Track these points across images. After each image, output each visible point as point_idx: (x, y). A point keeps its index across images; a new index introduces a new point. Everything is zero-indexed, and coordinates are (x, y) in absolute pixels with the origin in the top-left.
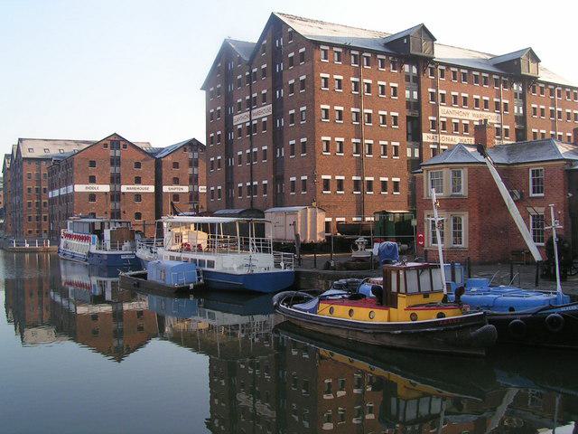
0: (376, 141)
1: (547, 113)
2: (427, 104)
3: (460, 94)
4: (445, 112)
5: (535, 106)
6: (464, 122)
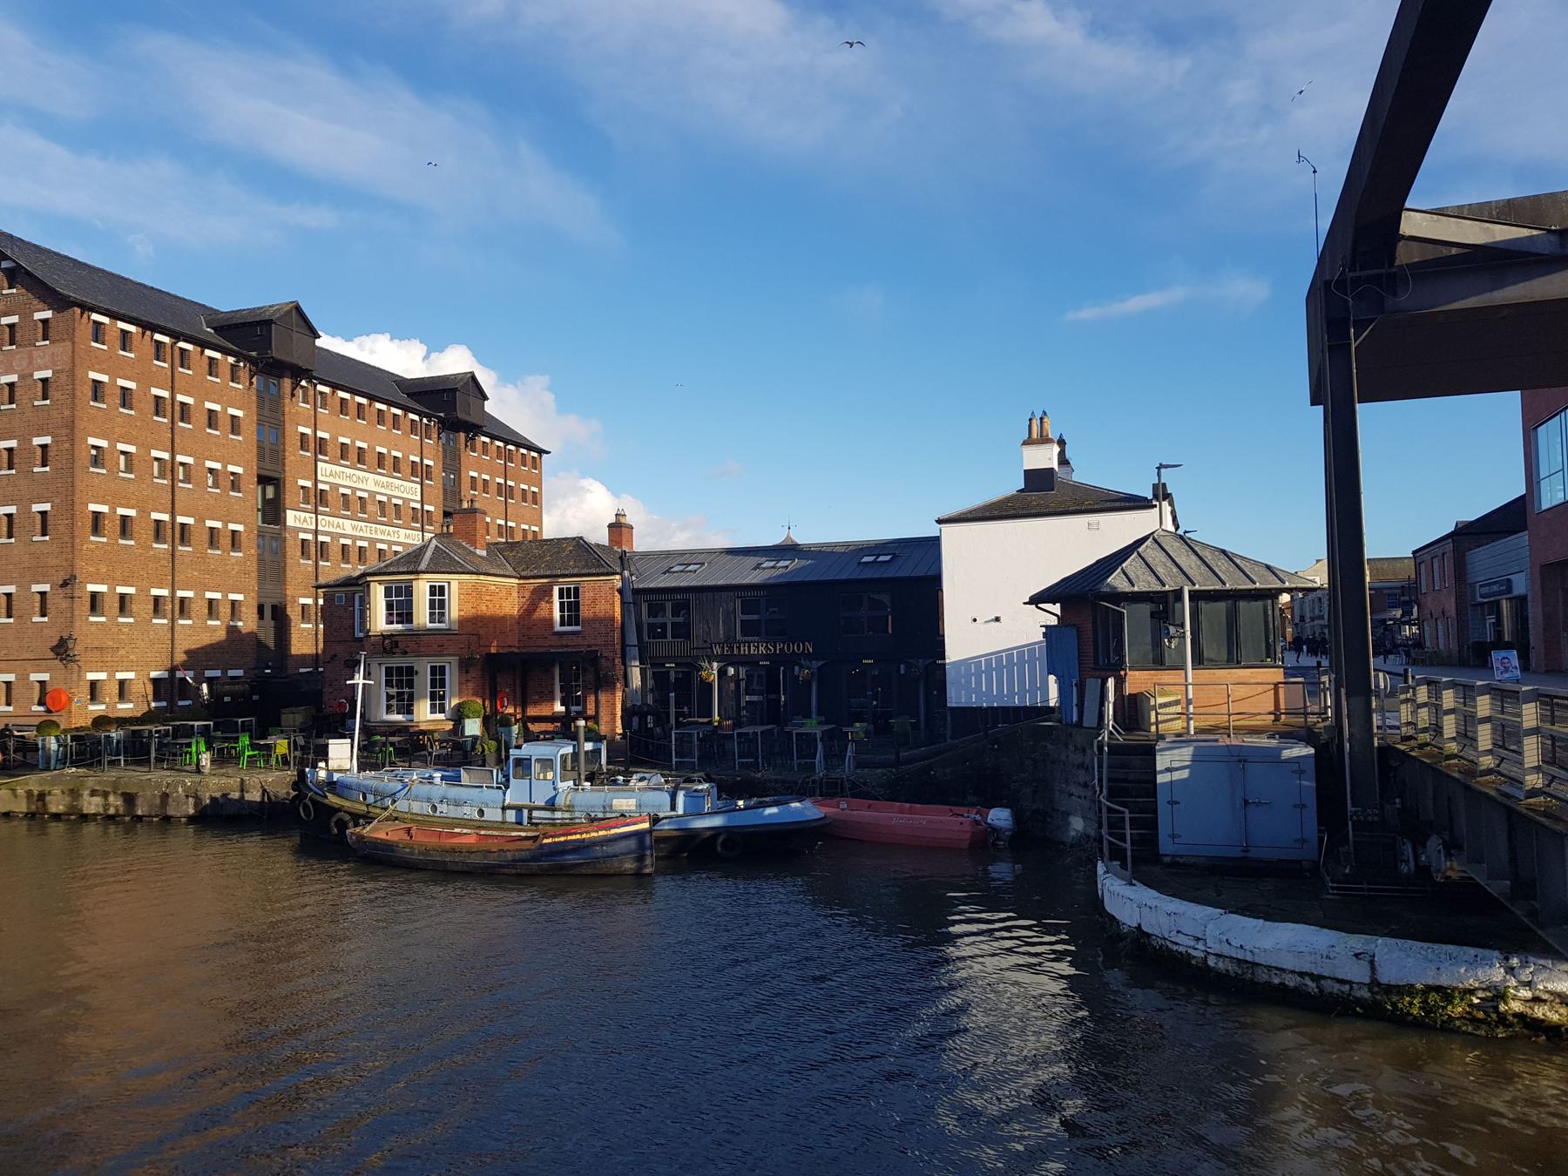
0: (201, 521)
1: (493, 488)
2: (295, 455)
3: (353, 442)
4: (331, 474)
5: (475, 474)
6: (359, 494)
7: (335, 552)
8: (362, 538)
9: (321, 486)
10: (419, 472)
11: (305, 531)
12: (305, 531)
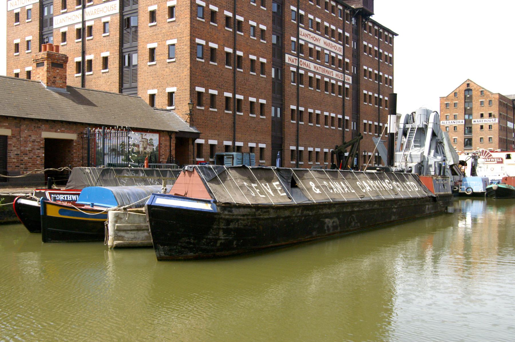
7: (306, 80)
8: (319, 74)
9: (301, 42)
10: (342, 38)
11: (293, 66)
12: (293, 66)
